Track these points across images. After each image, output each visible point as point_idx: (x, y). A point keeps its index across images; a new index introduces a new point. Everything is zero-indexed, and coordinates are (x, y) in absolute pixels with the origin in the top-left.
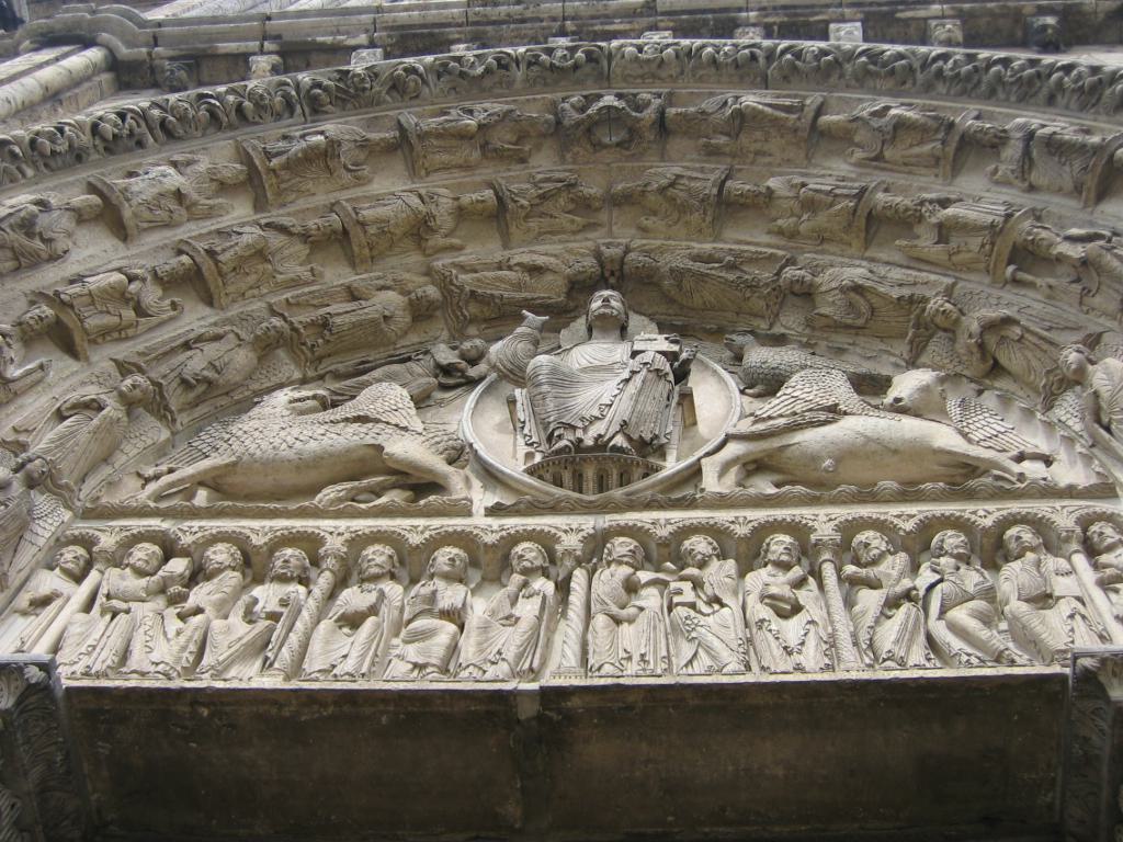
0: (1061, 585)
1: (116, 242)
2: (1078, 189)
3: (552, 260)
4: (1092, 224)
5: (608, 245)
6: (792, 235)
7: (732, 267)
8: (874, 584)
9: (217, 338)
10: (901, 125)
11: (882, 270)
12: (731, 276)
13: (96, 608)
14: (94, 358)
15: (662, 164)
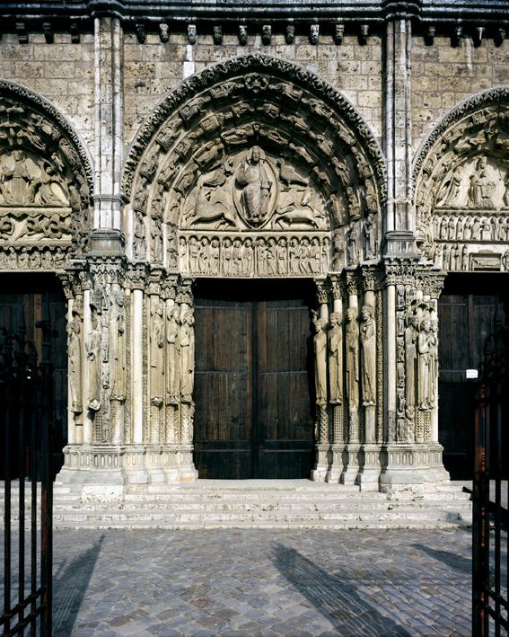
7: (279, 140)
12: (280, 142)
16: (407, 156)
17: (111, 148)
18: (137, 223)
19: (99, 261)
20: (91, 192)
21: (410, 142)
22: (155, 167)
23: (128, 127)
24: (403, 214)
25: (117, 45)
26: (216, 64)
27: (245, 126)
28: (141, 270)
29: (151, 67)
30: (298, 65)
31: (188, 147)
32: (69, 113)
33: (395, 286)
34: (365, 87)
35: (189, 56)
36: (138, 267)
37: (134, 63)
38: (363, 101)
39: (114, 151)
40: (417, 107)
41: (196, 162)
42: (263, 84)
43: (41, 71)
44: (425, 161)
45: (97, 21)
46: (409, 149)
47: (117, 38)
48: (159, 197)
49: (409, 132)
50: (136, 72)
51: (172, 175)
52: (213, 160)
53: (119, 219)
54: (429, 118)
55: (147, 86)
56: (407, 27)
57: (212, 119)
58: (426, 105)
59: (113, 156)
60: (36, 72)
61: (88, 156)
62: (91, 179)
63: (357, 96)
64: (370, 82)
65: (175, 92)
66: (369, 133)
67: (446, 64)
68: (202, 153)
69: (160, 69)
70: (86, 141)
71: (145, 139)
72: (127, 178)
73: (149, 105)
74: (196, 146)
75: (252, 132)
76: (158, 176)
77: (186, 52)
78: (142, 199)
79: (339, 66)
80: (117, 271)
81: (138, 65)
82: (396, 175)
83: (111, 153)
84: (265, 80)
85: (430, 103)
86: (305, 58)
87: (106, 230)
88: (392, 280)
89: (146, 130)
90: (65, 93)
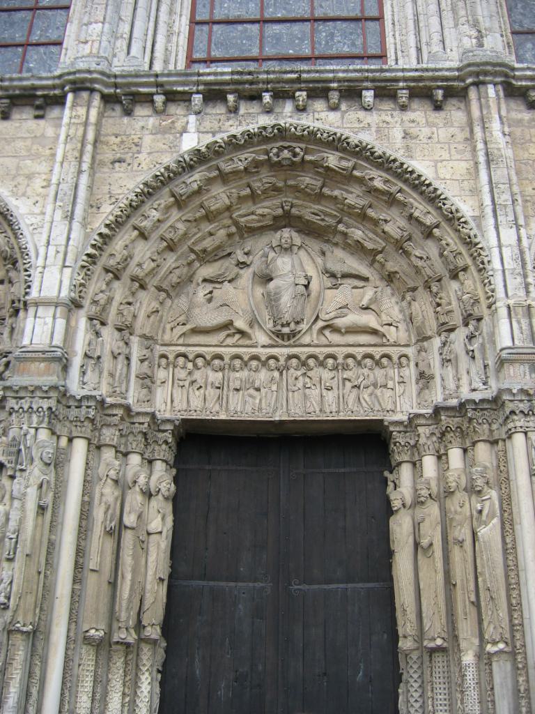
0: (390, 384)
1: (145, 241)
2: (422, 233)
3: (269, 210)
4: (423, 249)
5: (285, 202)
6: (342, 210)
7: (323, 220)
8: (349, 380)
9: (178, 267)
10: (377, 190)
11: (367, 232)
12: (323, 224)
13: (176, 385)
14: (149, 287)
15: (301, 174)
16: (519, 240)
17: (65, 236)
18: (91, 336)
19: (22, 394)
20: (27, 293)
21: (521, 221)
22: (127, 259)
23: (94, 210)
24: (524, 322)
26: (229, 134)
27: (266, 204)
28: (88, 407)
29: (136, 141)
30: (347, 133)
31: (181, 232)
32: (14, 194)
33: (526, 433)
34: (446, 156)
36: (85, 403)
37: (113, 138)
38: (443, 173)
40: (527, 179)
41: (192, 251)
42: (295, 155)
45: (70, 97)
46: (523, 231)
47: (94, 113)
48: (131, 300)
49: (519, 209)
50: (115, 147)
51: (154, 269)
52: (219, 247)
53: (63, 331)
55: (129, 161)
56: (497, 92)
57: (220, 196)
59: (67, 246)
61: (30, 247)
62: (29, 276)
63: (436, 166)
64: (453, 151)
65: (167, 168)
66: (457, 211)
68: (202, 238)
69: (149, 141)
70: (31, 228)
71: (117, 225)
72: (82, 275)
73: (127, 184)
74: (195, 230)
75: (280, 211)
76: (133, 269)
77: (188, 122)
78: (102, 302)
80: (50, 408)
81: (119, 139)
82: (506, 267)
83: (64, 242)
87: (40, 347)
88: (518, 424)
89: (120, 213)
90: (14, 172)
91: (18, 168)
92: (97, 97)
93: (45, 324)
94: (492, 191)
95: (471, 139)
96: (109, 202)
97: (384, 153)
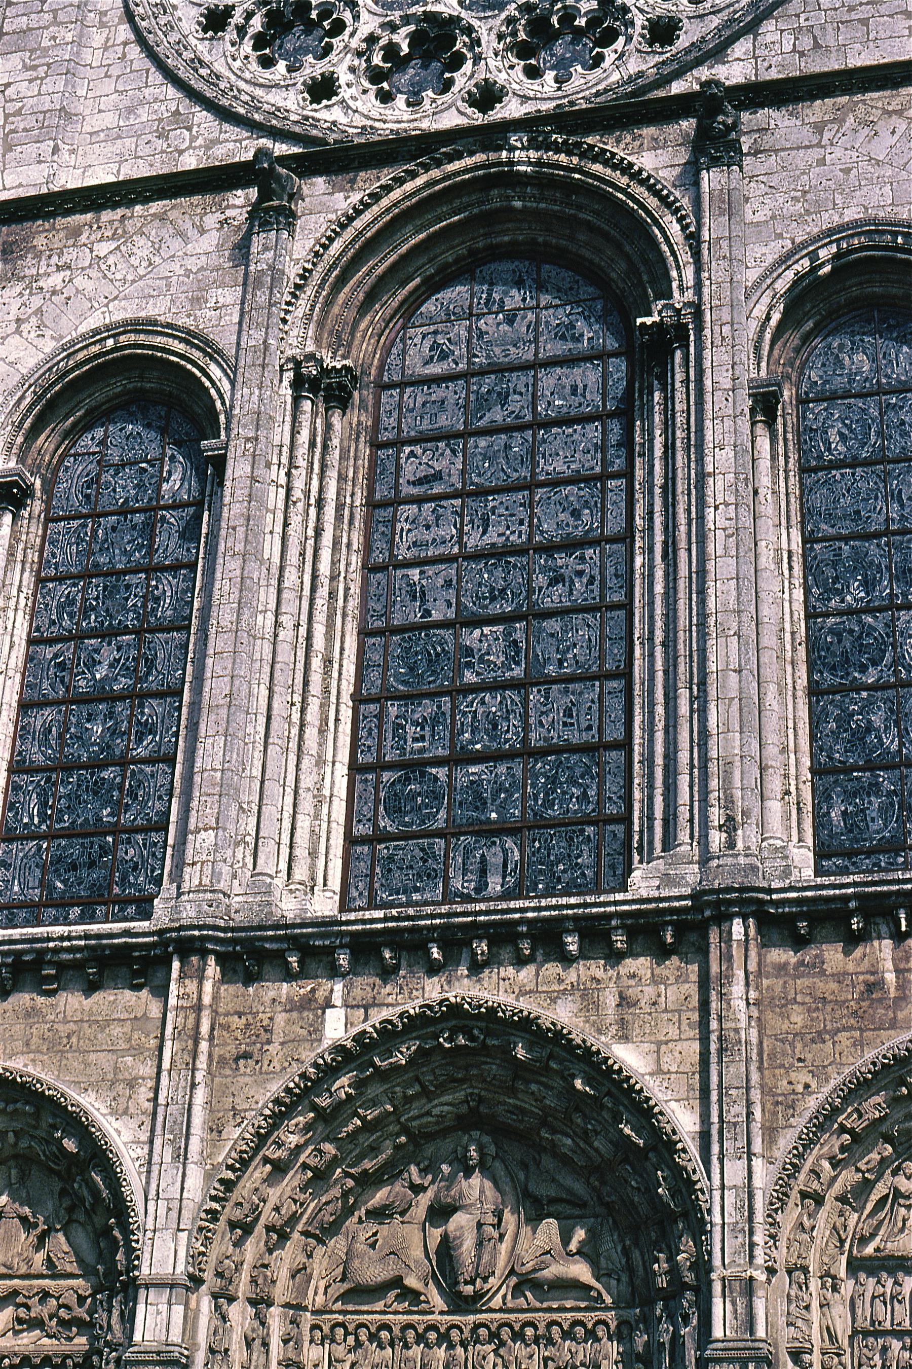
7: (521, 1121)
17: (179, 1184)
25: (207, 1000)
34: (673, 1032)
35: (337, 999)
39: (182, 1189)
40: (782, 1066)
43: (74, 1040)
44: (802, 1177)
50: (238, 1034)
54: (807, 1086)
58: (800, 1060)
60: (65, 1041)
63: (658, 1052)
64: (684, 1026)
66: (674, 1132)
67: (840, 977)
77: (332, 990)
79: (621, 996)
84: (476, 1032)
85: (809, 1056)
86: (556, 987)
87: (154, 1347)
89: (244, 1147)
90: (110, 1076)
91: (116, 1069)
92: (212, 960)
93: (159, 1313)
94: (720, 1101)
95: (704, 1006)
96: (232, 1123)
97: (584, 1041)
